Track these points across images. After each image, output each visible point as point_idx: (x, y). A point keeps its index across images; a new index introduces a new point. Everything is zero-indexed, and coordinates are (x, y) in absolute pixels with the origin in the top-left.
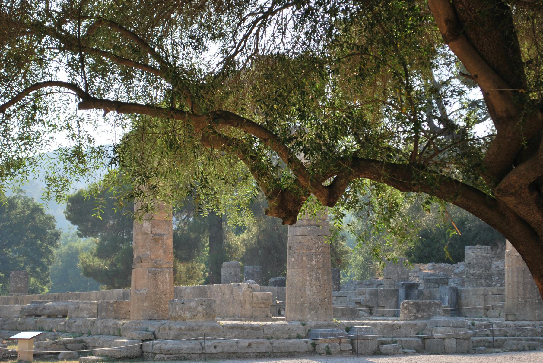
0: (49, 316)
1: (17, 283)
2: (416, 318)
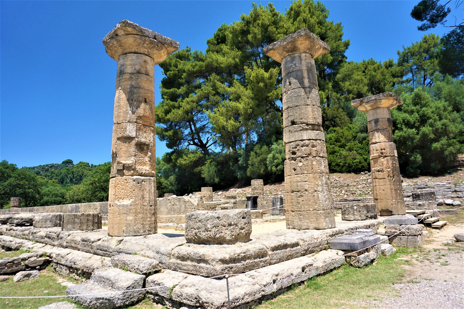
0: (18, 225)
1: (14, 203)
2: (367, 218)
